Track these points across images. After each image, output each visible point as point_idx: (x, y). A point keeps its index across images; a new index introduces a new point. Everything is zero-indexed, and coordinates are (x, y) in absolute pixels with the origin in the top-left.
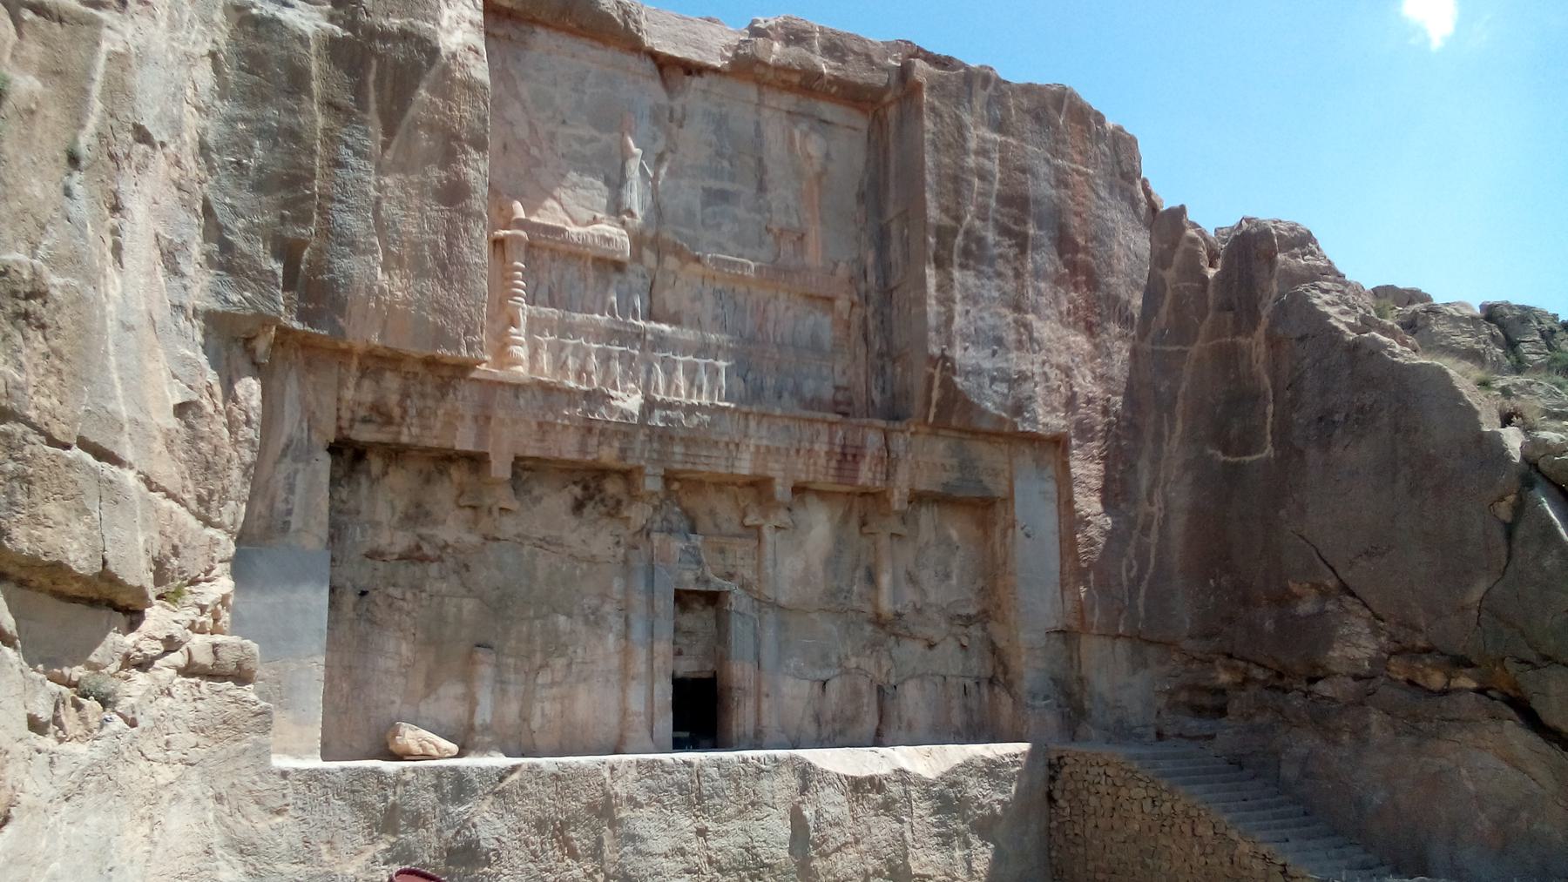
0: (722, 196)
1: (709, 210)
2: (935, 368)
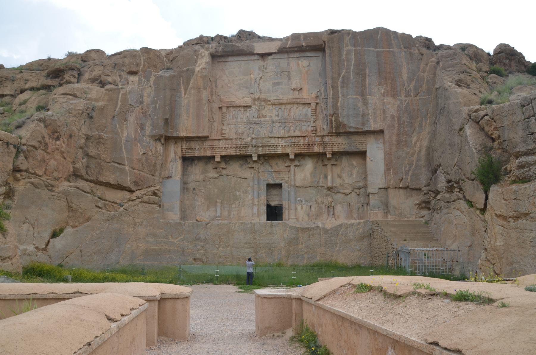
0: (278, 84)
1: (274, 88)
2: (332, 117)
